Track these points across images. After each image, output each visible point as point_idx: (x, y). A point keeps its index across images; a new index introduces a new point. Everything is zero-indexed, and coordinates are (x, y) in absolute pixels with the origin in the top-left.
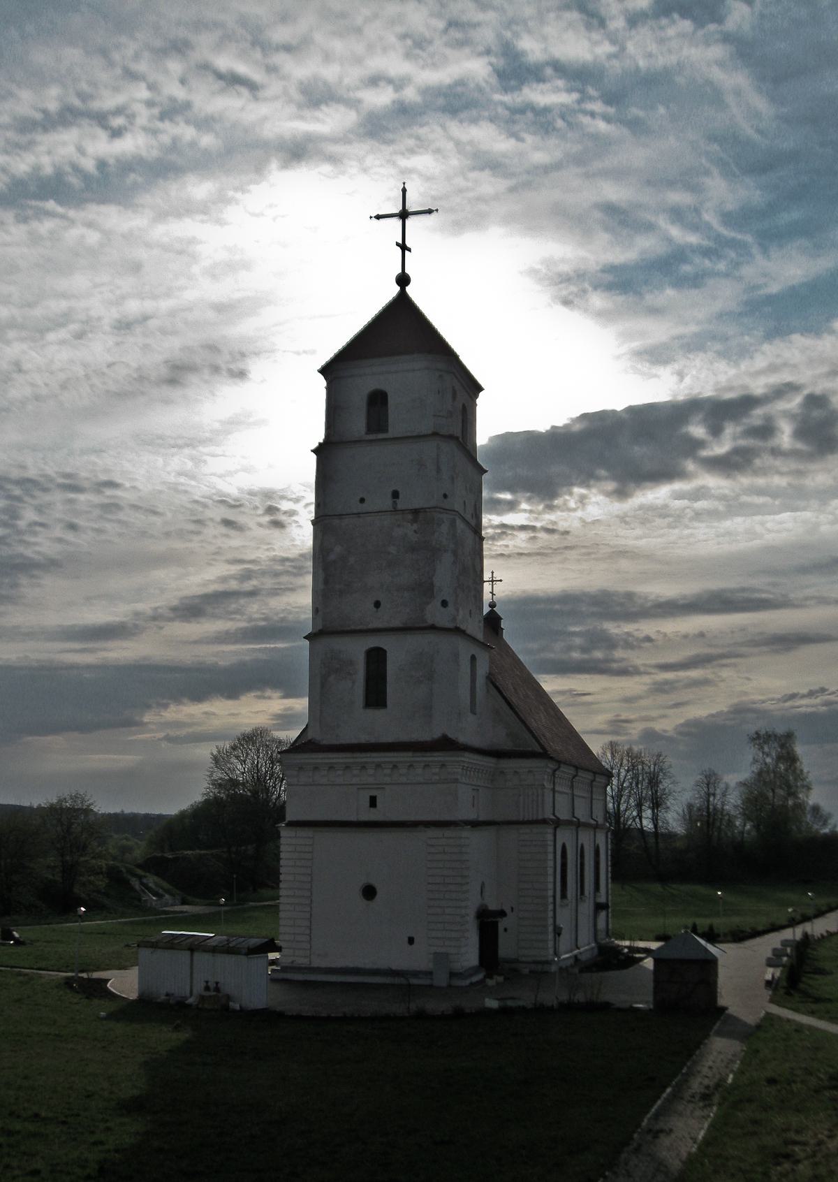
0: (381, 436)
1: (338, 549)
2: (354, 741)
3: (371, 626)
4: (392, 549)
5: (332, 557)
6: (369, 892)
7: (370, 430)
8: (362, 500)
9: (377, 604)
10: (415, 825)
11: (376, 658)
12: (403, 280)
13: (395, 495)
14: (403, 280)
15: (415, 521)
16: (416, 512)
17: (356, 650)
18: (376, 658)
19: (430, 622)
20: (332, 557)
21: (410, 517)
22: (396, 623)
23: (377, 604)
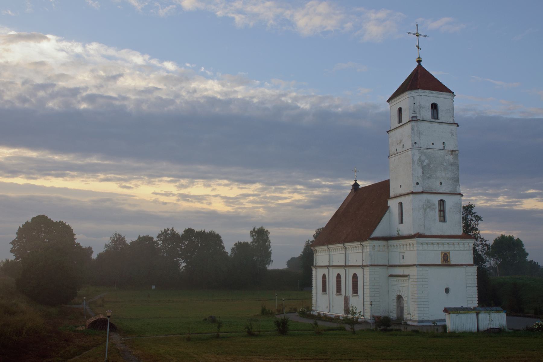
0: (437, 121)
1: (426, 161)
2: (436, 234)
3: (439, 192)
4: (445, 164)
5: (425, 164)
6: (447, 291)
7: (433, 118)
8: (433, 144)
9: (441, 183)
10: (462, 265)
11: (442, 202)
12: (419, 61)
13: (444, 143)
14: (419, 61)
15: (452, 154)
16: (452, 151)
17: (435, 199)
18: (442, 202)
19: (458, 192)
20: (425, 164)
21: (450, 152)
22: (447, 191)
23: (441, 183)
